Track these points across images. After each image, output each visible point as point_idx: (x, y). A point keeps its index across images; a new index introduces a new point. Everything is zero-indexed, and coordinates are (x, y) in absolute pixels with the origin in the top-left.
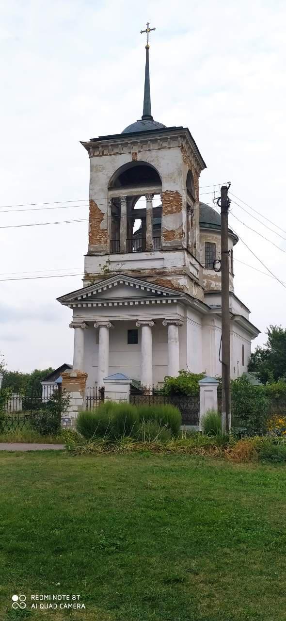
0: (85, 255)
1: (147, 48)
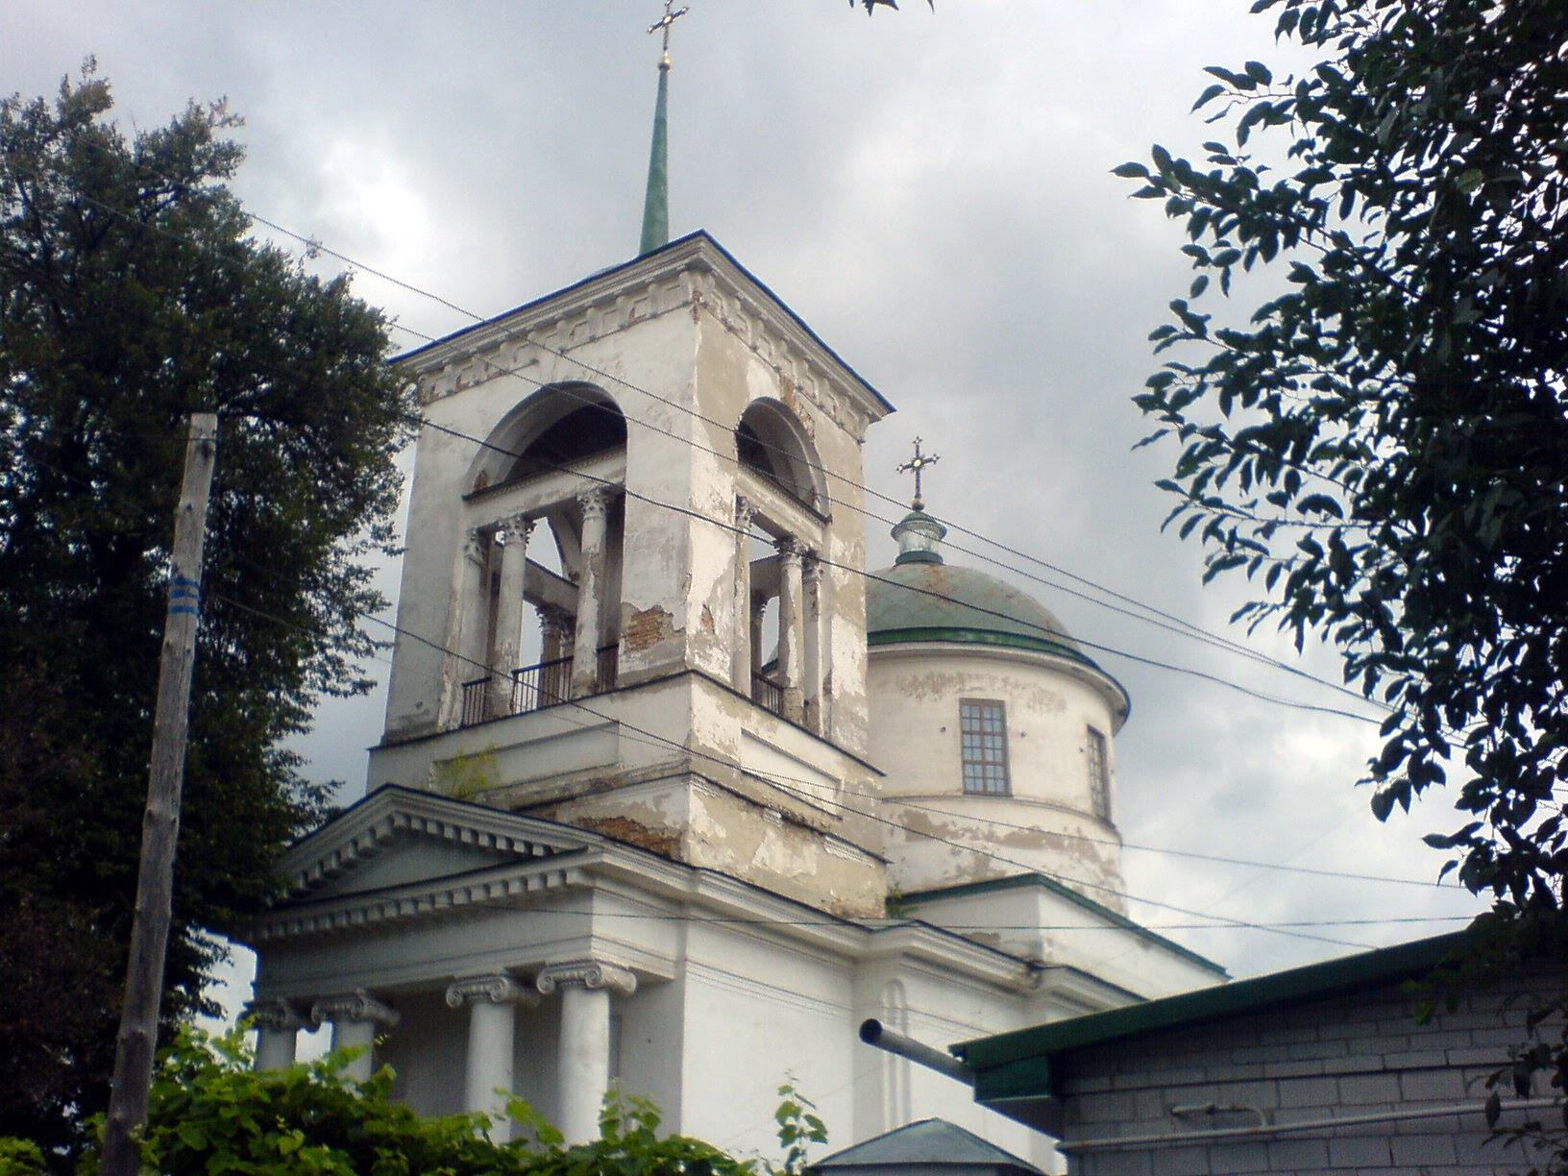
0: (372, 750)
1: (664, 68)
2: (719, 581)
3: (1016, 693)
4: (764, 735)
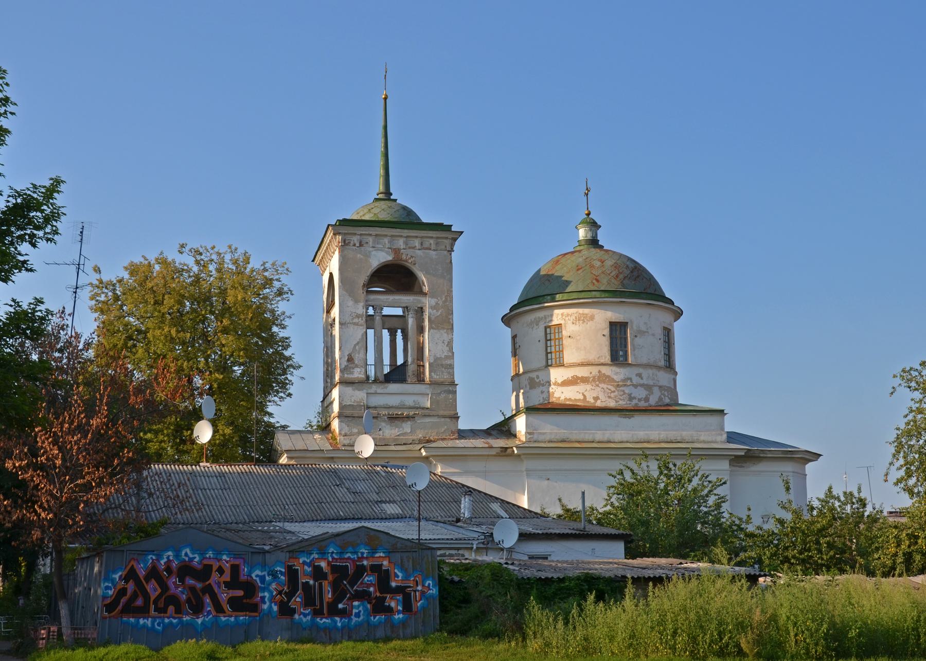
1: (385, 99)
2: (358, 343)
3: (567, 319)
4: (379, 391)
